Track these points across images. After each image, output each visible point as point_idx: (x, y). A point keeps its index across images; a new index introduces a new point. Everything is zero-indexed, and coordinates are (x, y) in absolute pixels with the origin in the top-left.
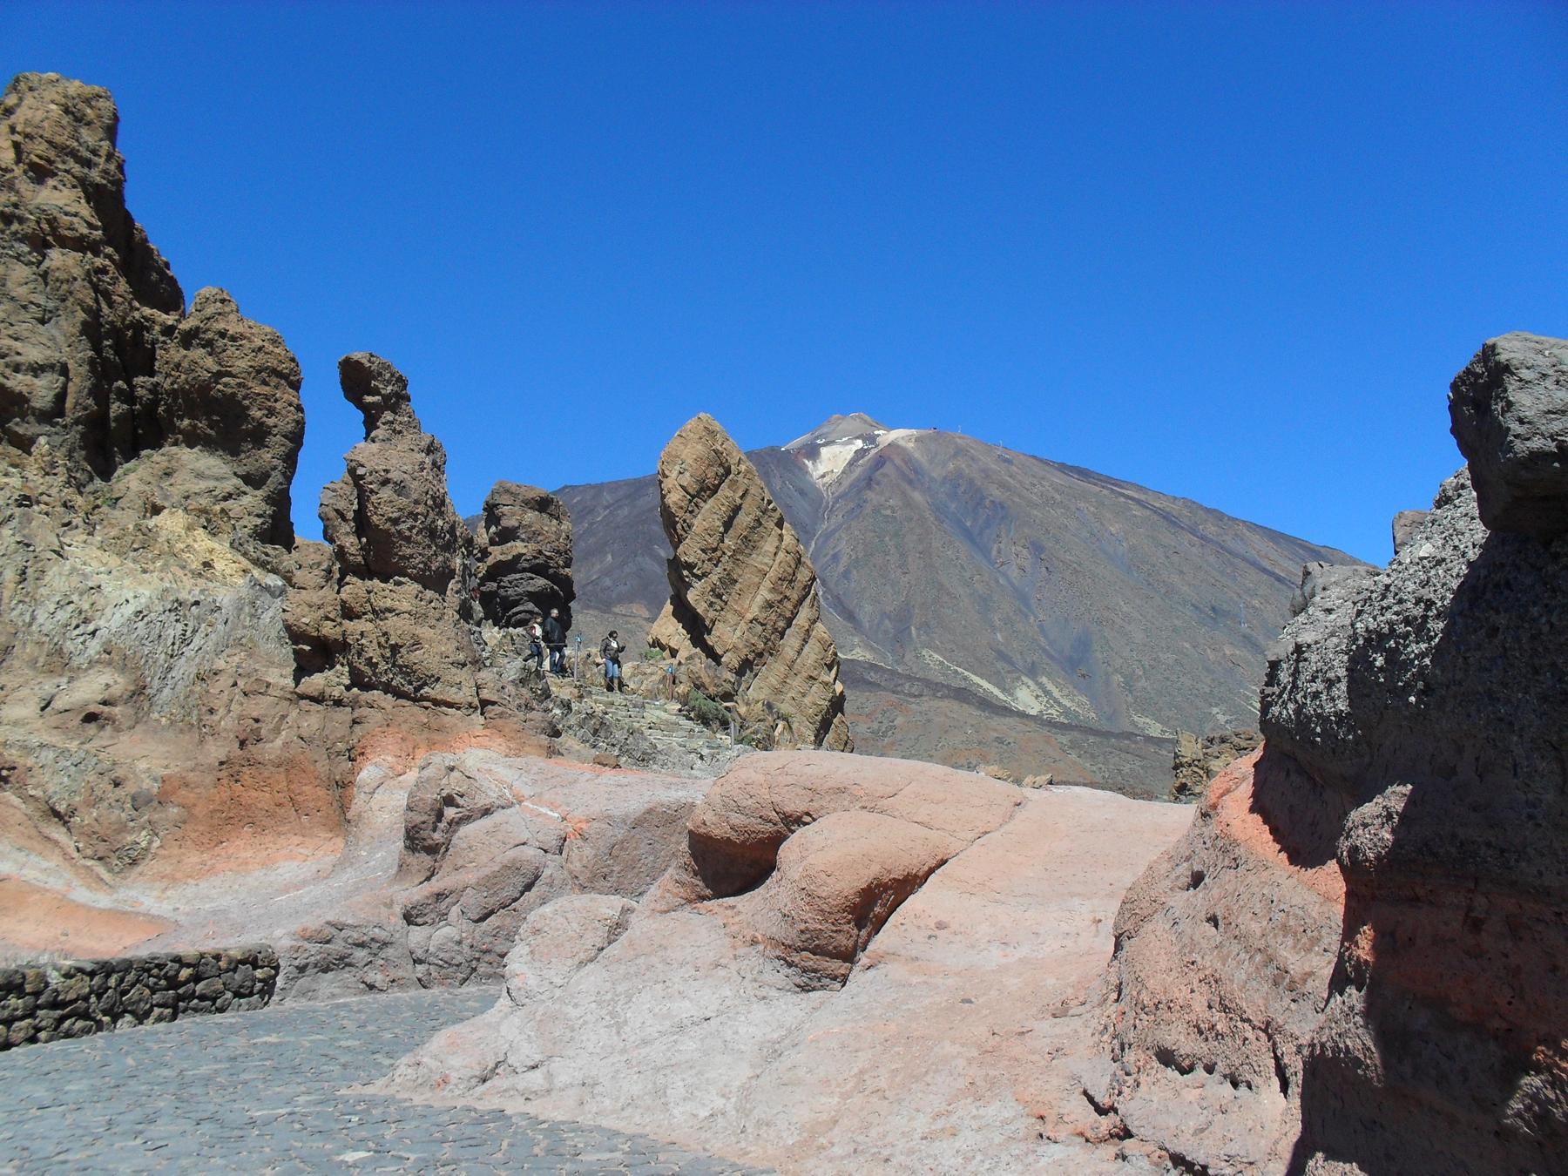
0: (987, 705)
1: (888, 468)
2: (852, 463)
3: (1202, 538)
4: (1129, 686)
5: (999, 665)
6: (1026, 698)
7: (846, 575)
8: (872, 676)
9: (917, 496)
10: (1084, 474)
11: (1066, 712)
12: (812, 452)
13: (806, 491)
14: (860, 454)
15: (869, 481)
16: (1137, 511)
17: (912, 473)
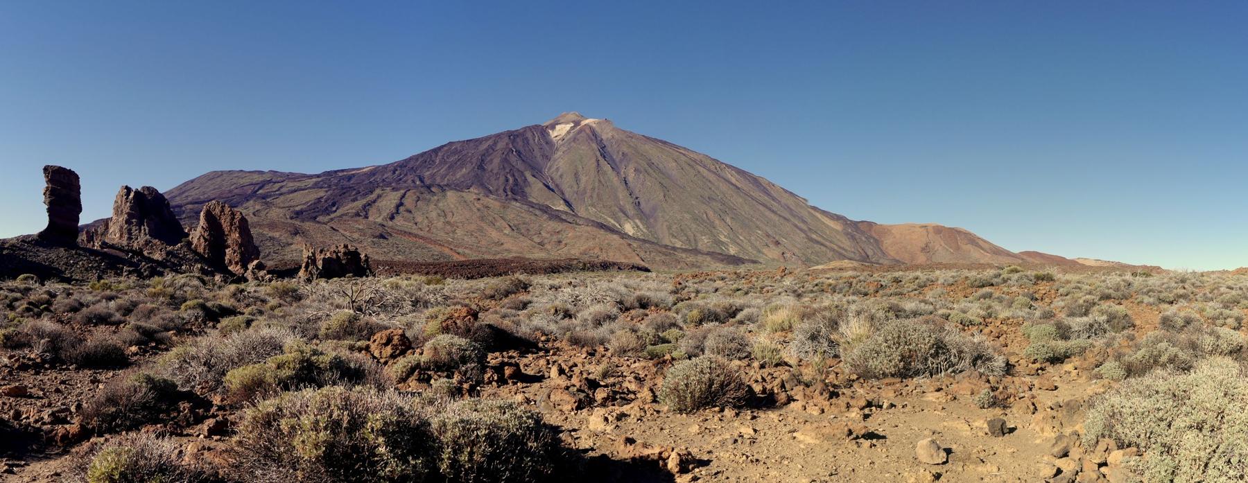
0: (612, 230)
1: (583, 134)
2: (569, 132)
3: (709, 170)
4: (669, 228)
5: (620, 214)
6: (629, 228)
7: (561, 176)
8: (564, 217)
9: (594, 146)
10: (665, 143)
11: (644, 234)
12: (553, 127)
13: (549, 143)
14: (572, 128)
15: (575, 139)
16: (683, 158)
17: (594, 135)
